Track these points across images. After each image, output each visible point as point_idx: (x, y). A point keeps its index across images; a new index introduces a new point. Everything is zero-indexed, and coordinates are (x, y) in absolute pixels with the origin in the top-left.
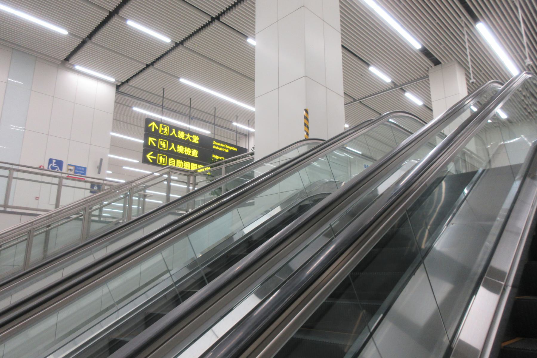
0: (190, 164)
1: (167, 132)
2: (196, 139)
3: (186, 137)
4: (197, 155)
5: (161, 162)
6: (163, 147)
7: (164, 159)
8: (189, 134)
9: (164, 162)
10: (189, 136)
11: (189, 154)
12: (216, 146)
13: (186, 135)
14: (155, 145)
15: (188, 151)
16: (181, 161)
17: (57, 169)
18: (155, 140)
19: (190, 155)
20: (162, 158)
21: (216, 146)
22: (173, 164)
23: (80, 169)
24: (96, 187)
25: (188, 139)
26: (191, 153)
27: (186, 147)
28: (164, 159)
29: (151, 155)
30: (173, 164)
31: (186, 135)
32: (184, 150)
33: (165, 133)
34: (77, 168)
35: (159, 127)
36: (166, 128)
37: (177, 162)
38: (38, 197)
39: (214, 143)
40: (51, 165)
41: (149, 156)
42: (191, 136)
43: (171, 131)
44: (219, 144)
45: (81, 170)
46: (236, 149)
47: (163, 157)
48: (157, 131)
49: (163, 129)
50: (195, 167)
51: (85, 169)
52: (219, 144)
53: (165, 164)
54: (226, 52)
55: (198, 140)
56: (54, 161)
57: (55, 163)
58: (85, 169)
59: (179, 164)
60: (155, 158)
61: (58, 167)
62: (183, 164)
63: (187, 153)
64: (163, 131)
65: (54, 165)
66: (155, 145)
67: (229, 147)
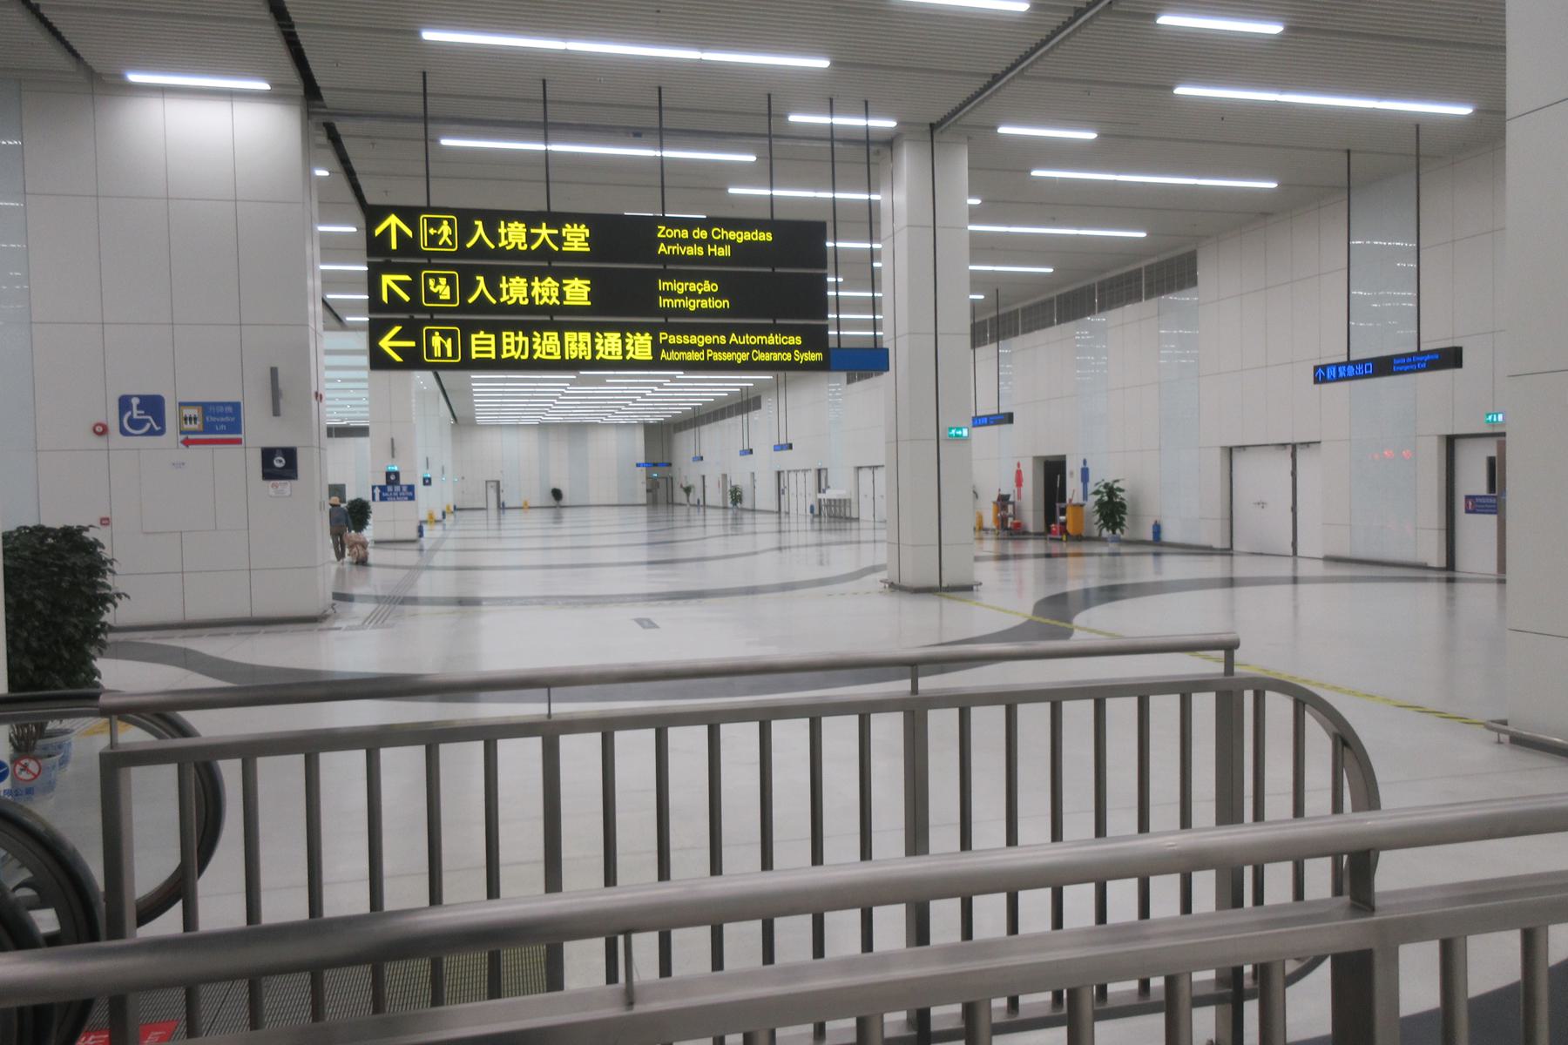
0: (561, 339)
1: (451, 237)
2: (577, 238)
3: (531, 238)
4: (586, 298)
5: (437, 353)
6: (441, 297)
7: (449, 344)
8: (544, 225)
9: (449, 354)
10: (544, 232)
11: (554, 301)
12: (668, 242)
13: (533, 231)
14: (407, 298)
15: (545, 291)
16: (521, 333)
17: (148, 425)
18: (407, 278)
19: (558, 303)
20: (440, 338)
21: (668, 242)
22: (489, 352)
23: (221, 409)
24: (281, 458)
25: (544, 239)
26: (562, 296)
27: (536, 279)
28: (450, 340)
29: (396, 338)
30: (489, 352)
31: (533, 231)
32: (530, 289)
33: (445, 245)
34: (211, 408)
35: (415, 229)
36: (445, 222)
37: (505, 340)
38: (108, 519)
39: (659, 235)
40: (129, 414)
41: (386, 343)
42: (556, 232)
43: (466, 231)
44: (685, 234)
45: (224, 414)
46: (769, 237)
47: (444, 334)
48: (407, 245)
49: (432, 231)
50: (582, 346)
51: (236, 407)
52: (685, 234)
53: (455, 355)
55: (587, 240)
56: (135, 401)
57: (139, 407)
58: (236, 407)
59: (512, 347)
60: (412, 344)
61: (150, 418)
62: (531, 343)
63: (541, 297)
64: (433, 240)
65: (136, 413)
66: (407, 298)
67: (732, 235)
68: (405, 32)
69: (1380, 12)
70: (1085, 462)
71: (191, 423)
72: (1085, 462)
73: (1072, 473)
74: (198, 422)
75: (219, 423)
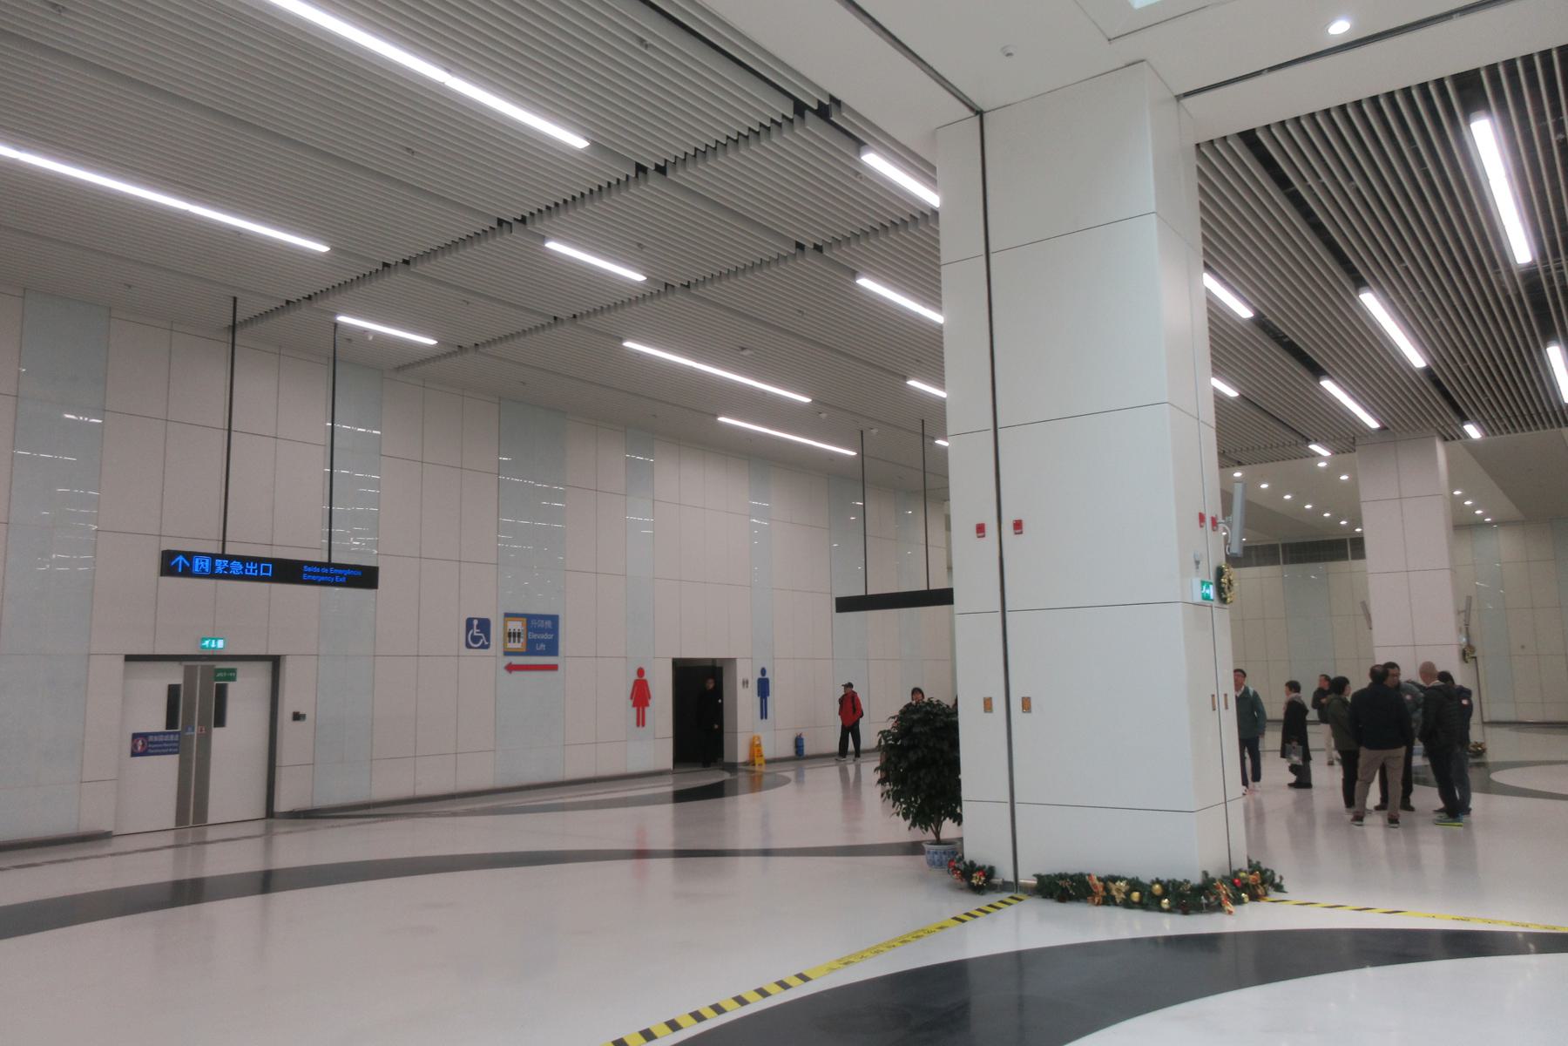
23: (541, 624)
40: (471, 632)
54: (1433, 413)
56: (476, 622)
57: (478, 627)
65: (475, 631)
68: (1437, 384)
69: (808, 323)
70: (763, 671)
71: (514, 641)
72: (763, 671)
73: (745, 683)
74: (522, 640)
75: (539, 641)
